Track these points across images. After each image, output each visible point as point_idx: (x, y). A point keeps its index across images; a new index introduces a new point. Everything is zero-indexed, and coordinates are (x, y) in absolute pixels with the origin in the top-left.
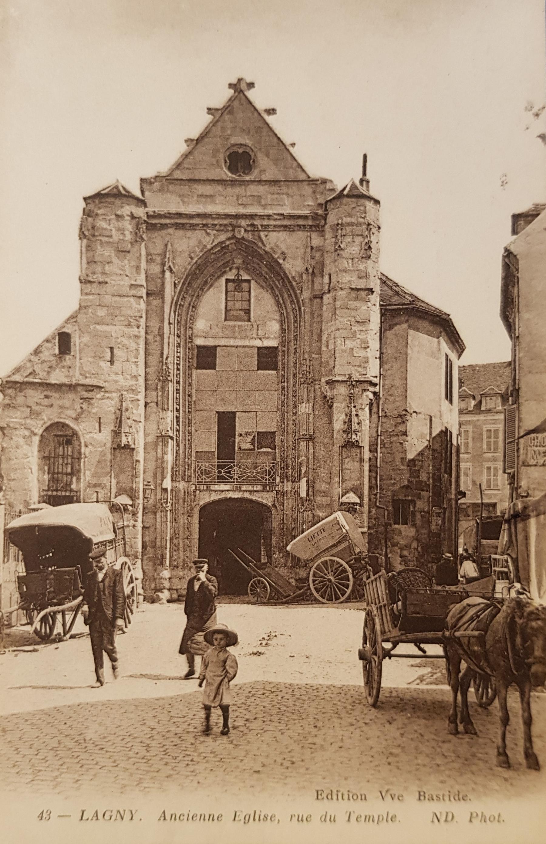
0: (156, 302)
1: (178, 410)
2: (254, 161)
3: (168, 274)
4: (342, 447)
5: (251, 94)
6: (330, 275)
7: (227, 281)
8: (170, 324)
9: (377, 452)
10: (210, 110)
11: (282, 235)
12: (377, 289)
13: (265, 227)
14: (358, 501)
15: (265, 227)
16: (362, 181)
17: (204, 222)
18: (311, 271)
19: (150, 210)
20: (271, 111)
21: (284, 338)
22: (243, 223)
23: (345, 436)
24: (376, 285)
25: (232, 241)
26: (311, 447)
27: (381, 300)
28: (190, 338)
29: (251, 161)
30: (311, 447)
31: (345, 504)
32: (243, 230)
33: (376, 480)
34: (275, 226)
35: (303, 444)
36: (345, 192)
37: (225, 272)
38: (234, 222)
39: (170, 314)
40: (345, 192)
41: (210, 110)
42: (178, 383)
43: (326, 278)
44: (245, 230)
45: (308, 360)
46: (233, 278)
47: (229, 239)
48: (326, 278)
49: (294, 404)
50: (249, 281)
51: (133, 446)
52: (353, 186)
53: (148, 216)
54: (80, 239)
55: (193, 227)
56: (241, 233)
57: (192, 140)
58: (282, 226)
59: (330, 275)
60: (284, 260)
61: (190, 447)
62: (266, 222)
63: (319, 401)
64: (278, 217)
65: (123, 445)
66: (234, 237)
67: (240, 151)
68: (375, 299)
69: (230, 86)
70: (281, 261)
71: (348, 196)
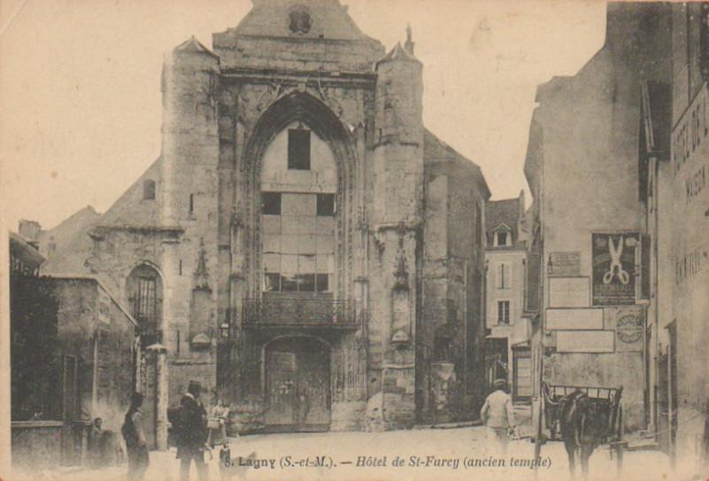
3: (239, 125)
6: (381, 130)
11: (339, 91)
14: (406, 339)
15: (323, 84)
16: (406, 44)
18: (364, 125)
19: (224, 64)
22: (305, 79)
31: (396, 342)
43: (377, 132)
44: (307, 86)
48: (377, 132)
49: (350, 248)
53: (222, 71)
56: (302, 88)
58: (337, 83)
62: (325, 79)
63: (373, 247)
66: (296, 92)
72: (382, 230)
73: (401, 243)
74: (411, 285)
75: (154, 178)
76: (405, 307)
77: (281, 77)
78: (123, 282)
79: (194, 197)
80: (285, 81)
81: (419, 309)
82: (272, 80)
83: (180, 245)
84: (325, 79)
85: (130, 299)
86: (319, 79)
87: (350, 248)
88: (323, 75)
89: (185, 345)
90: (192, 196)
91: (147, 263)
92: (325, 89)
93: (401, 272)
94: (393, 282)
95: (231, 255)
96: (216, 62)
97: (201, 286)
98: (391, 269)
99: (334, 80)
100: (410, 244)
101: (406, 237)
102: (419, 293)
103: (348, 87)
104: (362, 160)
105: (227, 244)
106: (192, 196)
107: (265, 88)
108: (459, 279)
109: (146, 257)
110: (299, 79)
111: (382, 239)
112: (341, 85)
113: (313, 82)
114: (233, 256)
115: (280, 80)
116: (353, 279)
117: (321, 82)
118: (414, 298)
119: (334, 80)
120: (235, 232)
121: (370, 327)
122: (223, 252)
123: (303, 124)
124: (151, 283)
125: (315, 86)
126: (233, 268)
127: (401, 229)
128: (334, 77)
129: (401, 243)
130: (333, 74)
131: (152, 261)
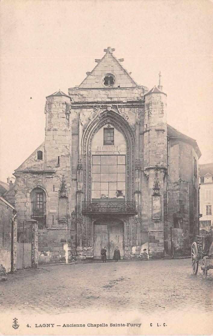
0: (76, 137)
2: (114, 81)
4: (153, 196)
5: (114, 54)
6: (146, 125)
7: (105, 129)
9: (167, 198)
10: (97, 61)
11: (127, 110)
12: (166, 130)
17: (95, 105)
20: (122, 60)
21: (128, 151)
22: (111, 105)
23: (154, 191)
25: (106, 112)
26: (140, 197)
27: (168, 135)
29: (113, 80)
30: (140, 197)
32: (110, 107)
33: (167, 210)
35: (136, 195)
36: (153, 91)
37: (103, 125)
39: (82, 142)
40: (153, 91)
41: (97, 61)
42: (85, 170)
44: (111, 108)
45: (138, 160)
46: (107, 127)
47: (105, 111)
49: (133, 178)
51: (67, 197)
52: (156, 88)
54: (45, 113)
56: (109, 109)
57: (89, 73)
59: (146, 125)
60: (127, 119)
61: (90, 197)
62: (119, 104)
66: (107, 110)
67: (109, 76)
68: (166, 133)
69: (105, 50)
70: (126, 120)
71: (154, 93)
72: (148, 169)
73: (156, 175)
74: (161, 193)
75: (42, 149)
76: (157, 203)
77: (99, 105)
78: (28, 195)
79: (60, 157)
80: (101, 106)
81: (165, 204)
82: (95, 106)
83: (54, 178)
84: (119, 104)
85: (32, 202)
86: (117, 104)
87: (133, 178)
88: (119, 102)
90: (59, 157)
91: (39, 187)
92: (120, 108)
93: (156, 188)
94: (152, 193)
95: (77, 182)
96: (70, 99)
97: (63, 196)
98: (152, 185)
99: (125, 104)
100: (161, 175)
101: (159, 172)
102: (165, 197)
103: (133, 106)
104: (137, 139)
105: (75, 178)
106: (59, 157)
107: (92, 110)
108: (185, 191)
109: (39, 184)
110: (108, 105)
111: (147, 173)
112: (128, 107)
113: (114, 106)
114: (78, 183)
115: (100, 106)
116: (134, 192)
117: (118, 105)
118: (163, 200)
119: (125, 104)
120: (79, 172)
121: (142, 213)
122: (74, 181)
123: (110, 125)
124: (41, 196)
125: (115, 107)
126: (78, 188)
127: (157, 169)
128: (124, 103)
129: (156, 175)
130: (124, 102)
131: (41, 186)
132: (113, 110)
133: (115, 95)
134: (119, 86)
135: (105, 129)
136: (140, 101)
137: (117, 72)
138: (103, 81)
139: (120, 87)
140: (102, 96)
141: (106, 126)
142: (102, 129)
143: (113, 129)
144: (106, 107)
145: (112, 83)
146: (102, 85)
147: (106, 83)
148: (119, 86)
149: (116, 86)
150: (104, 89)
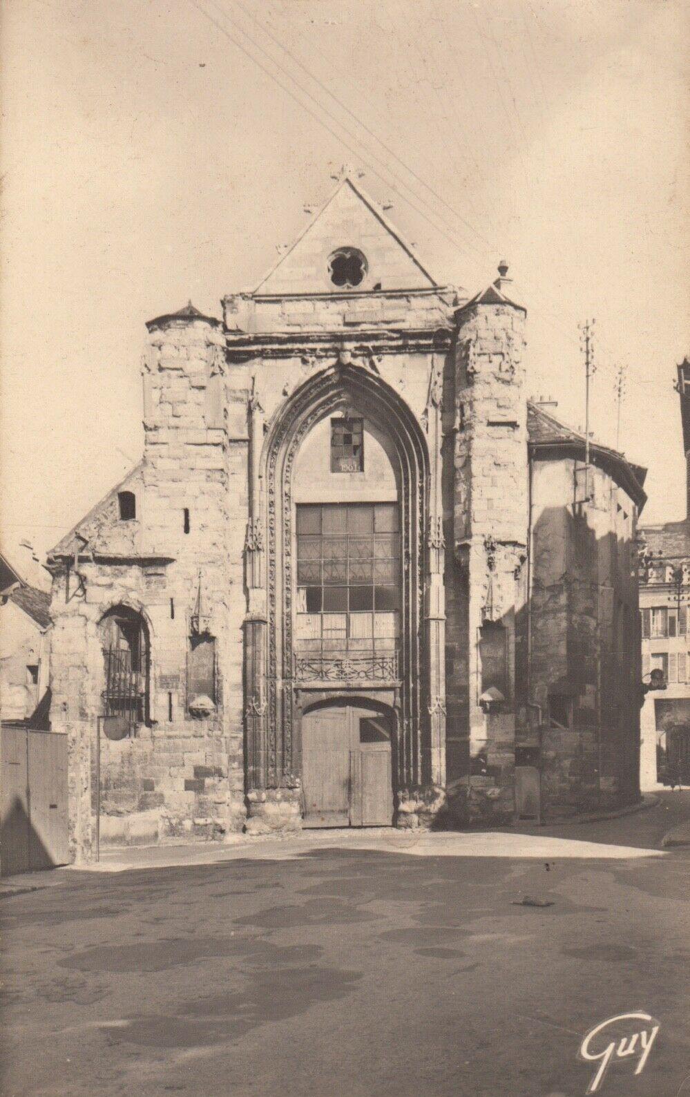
1: (272, 588)
3: (257, 413)
6: (462, 407)
7: (334, 422)
8: (260, 477)
12: (522, 420)
13: (378, 350)
22: (350, 346)
24: (521, 418)
28: (286, 494)
32: (348, 354)
34: (391, 348)
36: (478, 300)
38: (338, 345)
42: (272, 552)
50: (361, 420)
55: (285, 354)
64: (395, 335)
65: (200, 633)
67: (348, 256)
68: (522, 434)
80: (322, 350)
89: (179, 712)
125: (368, 353)
132: (358, 362)
133: (368, 311)
134: (378, 286)
135: (334, 422)
136: (442, 334)
137: (371, 242)
138: (329, 270)
139: (384, 287)
140: (329, 318)
141: (338, 414)
142: (326, 422)
143: (361, 420)
144: (338, 352)
145: (357, 278)
146: (325, 284)
147: (337, 279)
148: (378, 286)
149: (366, 284)
150: (333, 298)
